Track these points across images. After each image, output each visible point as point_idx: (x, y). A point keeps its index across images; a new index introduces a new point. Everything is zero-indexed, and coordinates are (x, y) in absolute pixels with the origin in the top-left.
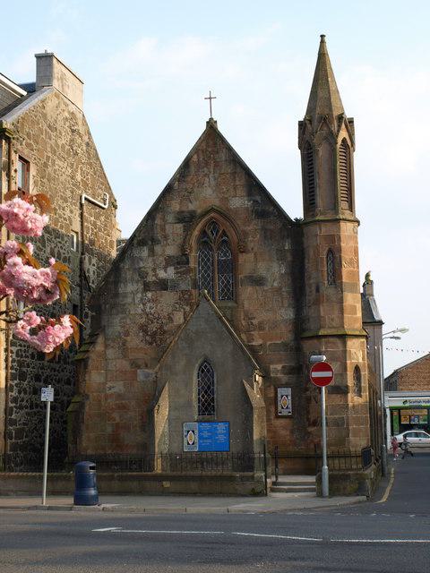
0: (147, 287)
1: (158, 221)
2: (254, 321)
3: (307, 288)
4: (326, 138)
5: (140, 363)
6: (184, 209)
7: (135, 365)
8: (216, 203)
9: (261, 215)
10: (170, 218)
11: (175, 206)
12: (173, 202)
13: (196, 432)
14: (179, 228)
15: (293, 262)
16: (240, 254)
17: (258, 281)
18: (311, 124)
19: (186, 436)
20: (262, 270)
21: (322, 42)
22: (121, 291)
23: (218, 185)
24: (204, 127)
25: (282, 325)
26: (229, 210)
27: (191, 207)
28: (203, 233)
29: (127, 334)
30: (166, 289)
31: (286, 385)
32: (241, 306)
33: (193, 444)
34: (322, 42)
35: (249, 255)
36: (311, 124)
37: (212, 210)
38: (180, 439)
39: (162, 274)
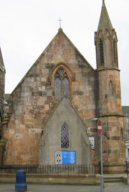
0: (33, 94)
1: (38, 67)
2: (78, 110)
3: (100, 97)
4: (108, 37)
5: (30, 126)
6: (49, 63)
7: (28, 127)
8: (63, 61)
9: (81, 66)
10: (44, 66)
11: (45, 61)
12: (44, 60)
13: (61, 155)
14: (47, 71)
15: (94, 86)
16: (73, 82)
17: (80, 93)
18: (101, 32)
19: (56, 157)
20: (81, 89)
21: (103, 3)
22: (22, 95)
23: (63, 54)
24: (57, 31)
25: (90, 111)
26: (68, 64)
27: (53, 62)
28: (57, 73)
29: (24, 113)
30: (41, 95)
31: (92, 136)
32: (73, 103)
33: (60, 161)
34: (103, 3)
35: (77, 82)
36: (101, 32)
37: (61, 63)
38: (54, 159)
39: (40, 89)
